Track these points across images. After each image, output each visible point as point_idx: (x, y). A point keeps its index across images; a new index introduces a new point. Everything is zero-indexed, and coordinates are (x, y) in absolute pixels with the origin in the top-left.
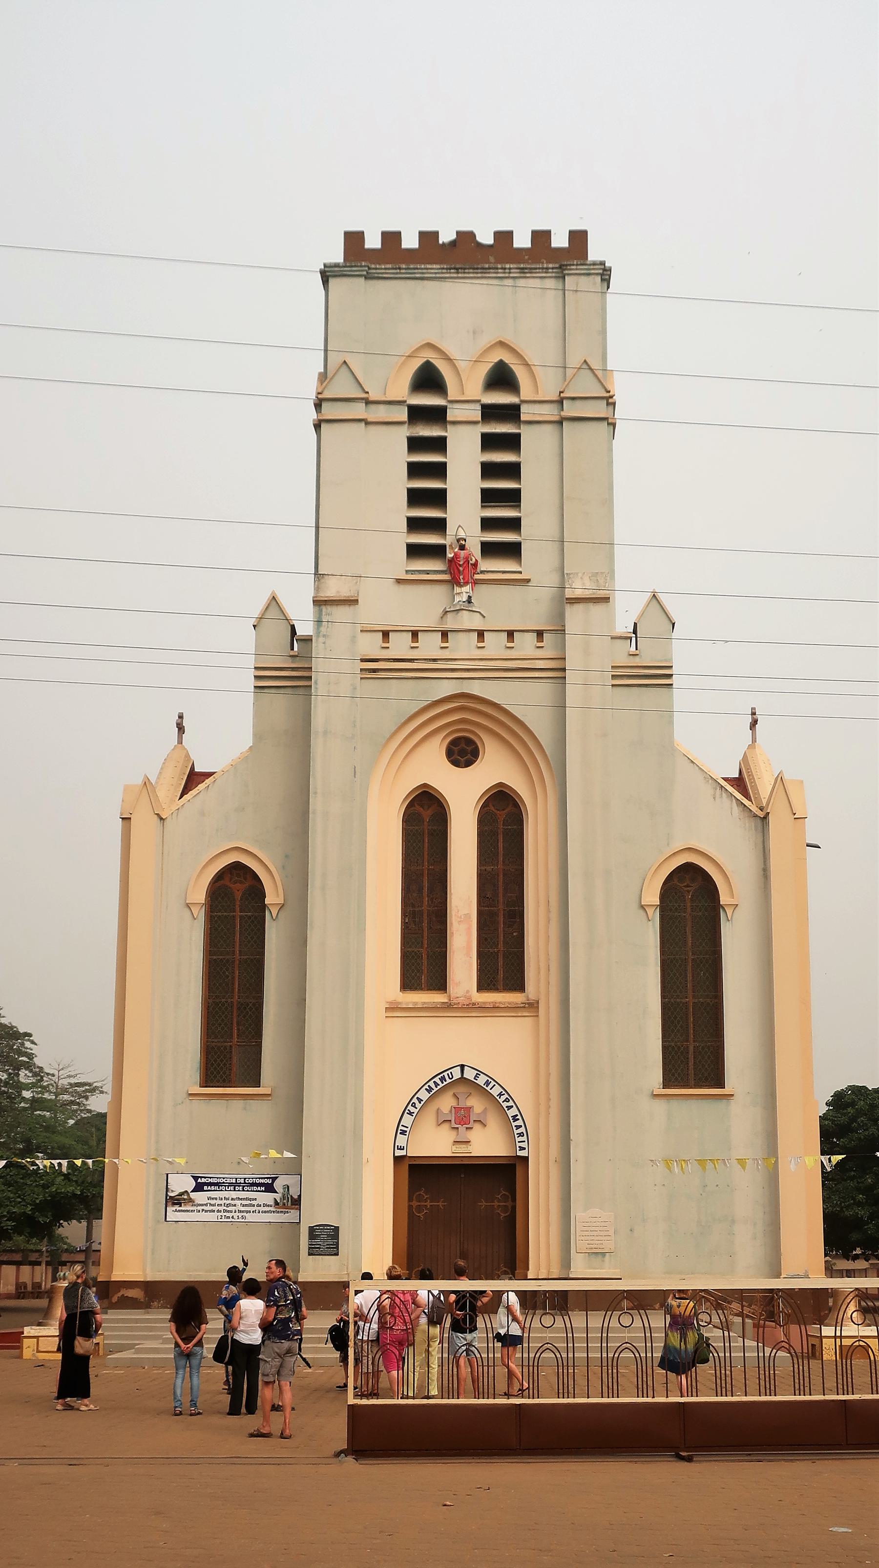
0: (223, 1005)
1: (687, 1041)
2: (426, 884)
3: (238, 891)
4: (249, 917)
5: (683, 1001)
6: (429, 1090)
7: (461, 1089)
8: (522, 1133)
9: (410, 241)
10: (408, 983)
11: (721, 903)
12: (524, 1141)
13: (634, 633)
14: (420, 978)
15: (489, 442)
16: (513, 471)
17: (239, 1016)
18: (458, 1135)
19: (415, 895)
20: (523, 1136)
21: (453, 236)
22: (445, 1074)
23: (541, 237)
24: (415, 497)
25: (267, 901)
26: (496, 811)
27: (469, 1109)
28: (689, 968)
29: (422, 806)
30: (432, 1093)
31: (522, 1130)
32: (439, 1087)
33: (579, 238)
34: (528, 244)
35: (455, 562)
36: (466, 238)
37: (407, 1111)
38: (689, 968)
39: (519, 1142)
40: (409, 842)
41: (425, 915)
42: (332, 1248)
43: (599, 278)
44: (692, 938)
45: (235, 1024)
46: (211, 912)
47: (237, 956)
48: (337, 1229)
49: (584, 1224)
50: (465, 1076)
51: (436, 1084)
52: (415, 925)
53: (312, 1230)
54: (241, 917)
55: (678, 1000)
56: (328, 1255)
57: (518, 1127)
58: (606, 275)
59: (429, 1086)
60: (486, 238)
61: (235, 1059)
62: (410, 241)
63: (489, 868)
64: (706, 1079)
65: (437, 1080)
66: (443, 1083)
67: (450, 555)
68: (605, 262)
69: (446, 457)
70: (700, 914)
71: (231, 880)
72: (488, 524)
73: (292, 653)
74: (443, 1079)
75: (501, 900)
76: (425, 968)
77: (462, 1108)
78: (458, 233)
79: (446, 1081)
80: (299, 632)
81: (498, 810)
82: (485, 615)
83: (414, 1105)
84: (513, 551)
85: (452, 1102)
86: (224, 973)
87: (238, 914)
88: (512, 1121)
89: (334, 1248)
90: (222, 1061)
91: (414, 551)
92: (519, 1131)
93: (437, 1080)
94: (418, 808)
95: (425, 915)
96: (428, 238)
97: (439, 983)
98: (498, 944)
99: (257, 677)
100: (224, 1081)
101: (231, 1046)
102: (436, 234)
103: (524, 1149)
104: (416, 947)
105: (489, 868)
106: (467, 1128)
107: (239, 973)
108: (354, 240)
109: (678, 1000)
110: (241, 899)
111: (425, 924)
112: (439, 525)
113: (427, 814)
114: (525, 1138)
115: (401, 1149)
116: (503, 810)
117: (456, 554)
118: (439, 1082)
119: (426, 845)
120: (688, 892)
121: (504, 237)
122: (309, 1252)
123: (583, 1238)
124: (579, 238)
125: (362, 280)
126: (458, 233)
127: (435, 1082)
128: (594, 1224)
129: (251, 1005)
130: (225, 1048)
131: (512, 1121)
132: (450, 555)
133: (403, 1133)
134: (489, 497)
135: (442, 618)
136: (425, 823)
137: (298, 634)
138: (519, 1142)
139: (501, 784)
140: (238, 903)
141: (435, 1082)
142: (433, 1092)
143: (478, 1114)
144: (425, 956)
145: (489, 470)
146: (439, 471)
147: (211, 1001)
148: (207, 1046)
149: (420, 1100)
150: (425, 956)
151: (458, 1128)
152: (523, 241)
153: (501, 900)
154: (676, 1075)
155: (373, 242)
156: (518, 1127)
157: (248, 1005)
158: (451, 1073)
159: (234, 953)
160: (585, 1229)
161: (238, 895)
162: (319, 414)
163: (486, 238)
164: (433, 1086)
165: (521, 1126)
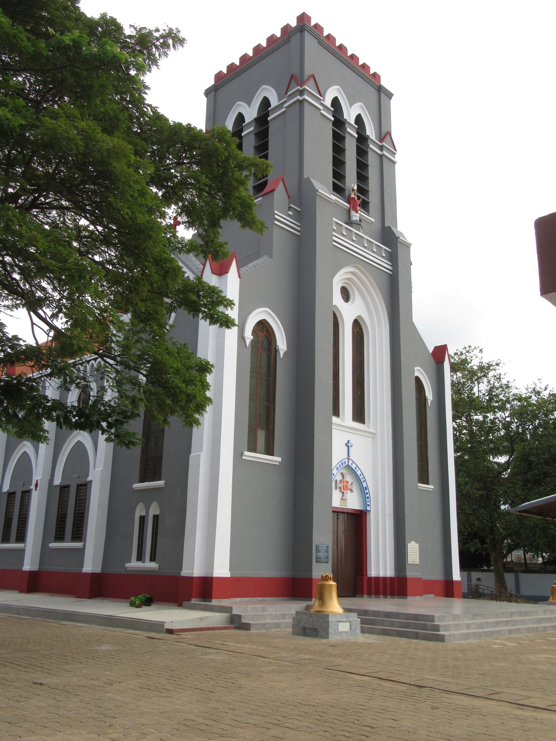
22: (343, 461)
31: (368, 496)
39: (368, 501)
48: (328, 546)
51: (340, 467)
53: (317, 547)
57: (367, 493)
65: (340, 463)
74: (342, 464)
93: (340, 463)
123: (410, 556)
138: (368, 501)
151: (343, 492)
156: (367, 493)
160: (411, 551)
164: (339, 467)
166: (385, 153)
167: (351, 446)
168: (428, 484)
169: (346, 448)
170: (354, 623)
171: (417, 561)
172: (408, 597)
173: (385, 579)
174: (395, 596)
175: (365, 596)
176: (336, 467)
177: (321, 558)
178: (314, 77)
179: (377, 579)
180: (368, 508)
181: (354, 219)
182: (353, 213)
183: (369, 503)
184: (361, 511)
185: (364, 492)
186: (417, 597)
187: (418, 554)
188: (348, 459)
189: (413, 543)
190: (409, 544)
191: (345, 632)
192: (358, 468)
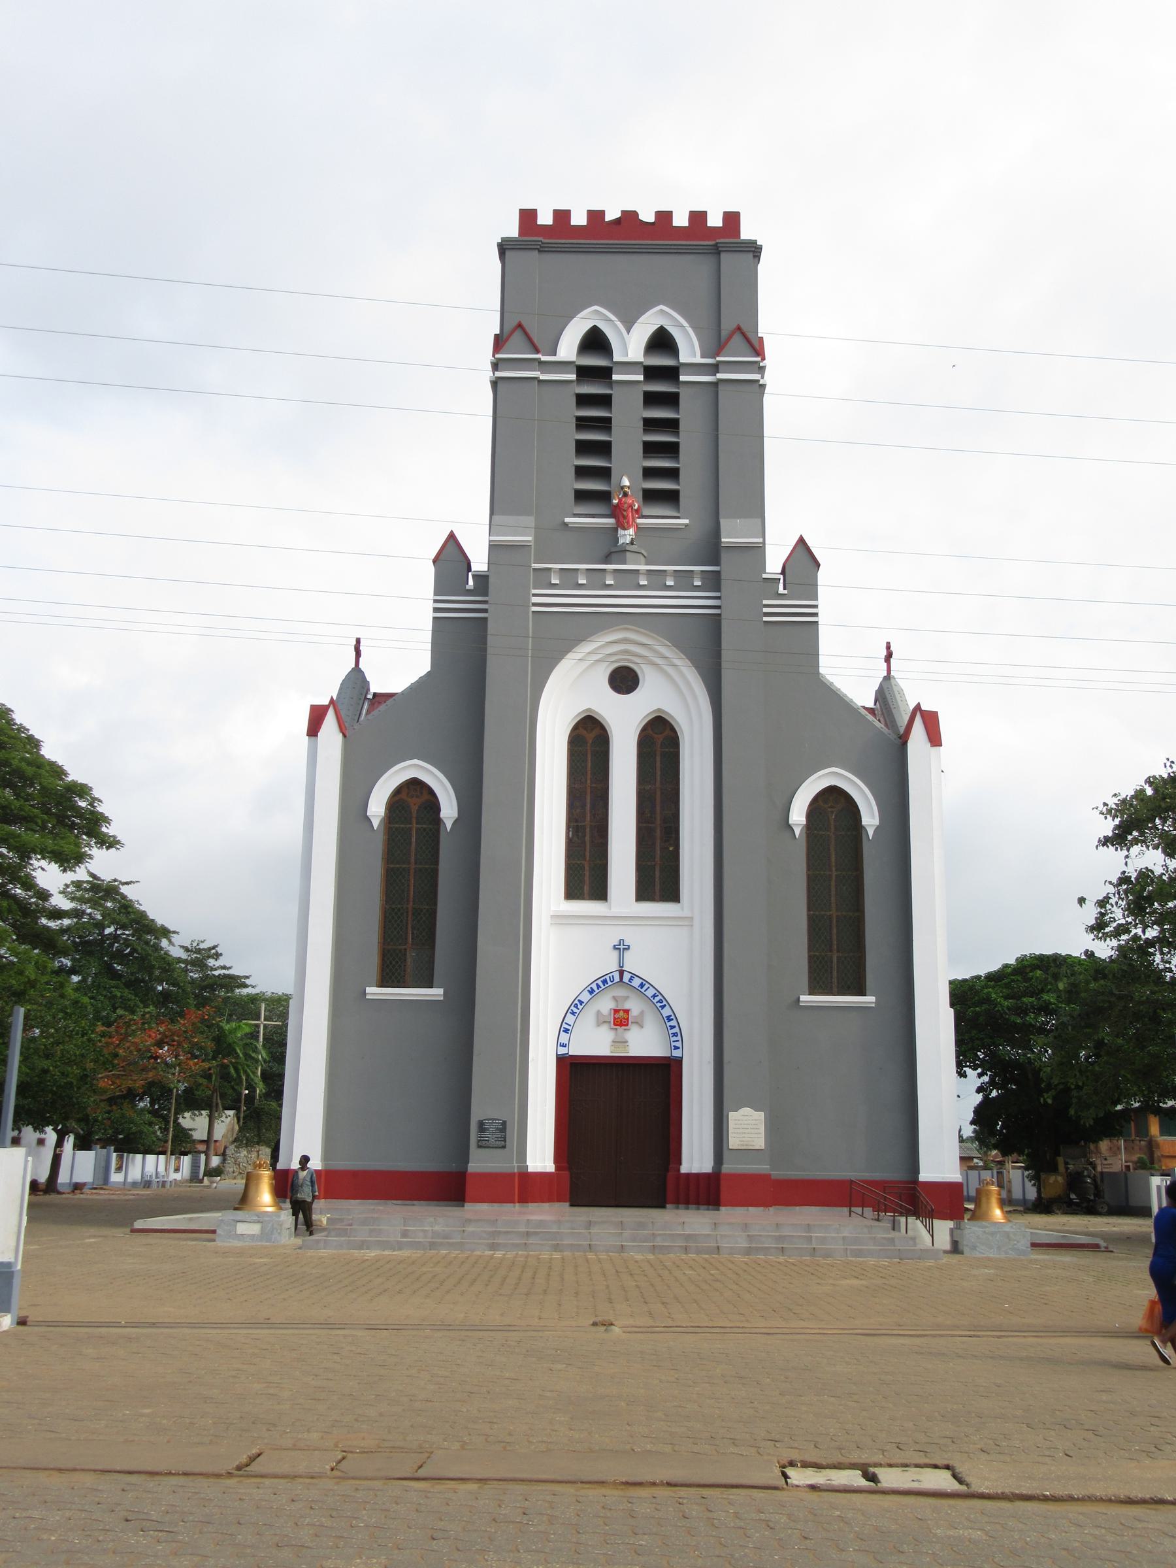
0: (399, 910)
1: (831, 951)
2: (588, 800)
3: (415, 805)
4: (425, 830)
5: (828, 913)
6: (592, 991)
7: (620, 992)
8: (677, 1033)
9: (579, 219)
10: (573, 891)
11: (863, 823)
12: (678, 1041)
13: (781, 574)
14: (582, 888)
15: (651, 399)
16: (672, 425)
17: (414, 920)
18: (616, 1035)
19: (578, 811)
20: (677, 1036)
21: (619, 215)
22: (607, 977)
23: (698, 218)
24: (583, 448)
25: (442, 815)
26: (656, 736)
27: (627, 1012)
28: (833, 883)
29: (586, 729)
30: (593, 995)
31: (676, 1030)
32: (600, 989)
33: (732, 220)
34: (685, 223)
35: (619, 508)
36: (629, 217)
37: (570, 1011)
38: (833, 883)
39: (674, 1041)
40: (573, 761)
41: (588, 830)
42: (499, 1141)
43: (751, 255)
44: (835, 855)
45: (410, 926)
46: (389, 823)
47: (413, 866)
48: (504, 1123)
49: (736, 1122)
50: (624, 980)
51: (598, 987)
52: (578, 838)
54: (417, 829)
55: (823, 913)
56: (496, 1147)
57: (672, 1027)
58: (757, 252)
59: (591, 988)
60: (648, 216)
61: (409, 960)
62: (579, 219)
63: (648, 787)
64: (849, 987)
65: (599, 982)
66: (604, 985)
67: (615, 501)
68: (756, 240)
69: (611, 413)
70: (843, 833)
71: (408, 794)
72: (649, 473)
73: (467, 587)
74: (605, 982)
75: (658, 817)
76: (587, 878)
77: (620, 1010)
78: (622, 211)
79: (607, 984)
80: (475, 567)
81: (656, 733)
82: (646, 555)
83: (576, 1006)
84: (671, 498)
85: (612, 1005)
86: (400, 881)
87: (415, 825)
88: (666, 1021)
89: (503, 1141)
90: (397, 962)
91: (582, 496)
92: (674, 1031)
94: (582, 732)
95: (588, 830)
96: (595, 216)
97: (600, 893)
98: (655, 858)
99: (436, 610)
100: (399, 982)
101: (405, 949)
102: (601, 213)
103: (678, 1048)
104: (579, 860)
105: (648, 787)
106: (625, 1029)
107: (414, 881)
108: (528, 217)
109: (823, 913)
110: (417, 813)
111: (587, 838)
112: (604, 474)
113: (590, 736)
114: (679, 1038)
115: (563, 1046)
116: (661, 733)
117: (620, 500)
118: (601, 984)
119: (589, 765)
120: (832, 812)
121: (664, 217)
122: (478, 1144)
124: (732, 220)
125: (537, 251)
126: (622, 211)
127: (597, 985)
128: (746, 1122)
129: (424, 911)
130: (400, 951)
131: (666, 1021)
132: (615, 501)
133: (566, 1031)
134: (650, 449)
135: (607, 557)
136: (589, 745)
137: (472, 570)
138: (674, 1041)
139: (659, 710)
140: (414, 814)
141: (597, 985)
142: (595, 993)
143: (635, 1017)
144: (587, 868)
145: (650, 424)
146: (605, 424)
147: (388, 907)
148: (384, 949)
149: (581, 1002)
150: (587, 868)
152: (681, 220)
153: (658, 817)
154: (821, 983)
155: (545, 218)
156: (672, 1027)
157: (422, 911)
158: (613, 976)
159: (409, 863)
160: (737, 1126)
161: (414, 809)
162: (496, 372)
163: (648, 216)
164: (595, 987)
165: (674, 1027)
166: (720, 376)
167: (624, 949)
168: (865, 996)
169: (616, 953)
170: (270, 1225)
171: (759, 1143)
172: (723, 1209)
173: (698, 1176)
174: (711, 1207)
175: (667, 1205)
176: (589, 988)
177: (488, 1141)
178: (520, 326)
179: (688, 1175)
180: (676, 1053)
181: (621, 541)
182: (621, 532)
183: (677, 1044)
184: (669, 1057)
185: (671, 1024)
186: (750, 1208)
187: (762, 1130)
188: (621, 973)
189: (746, 1111)
190: (731, 1114)
191: (249, 1235)
192: (647, 985)
